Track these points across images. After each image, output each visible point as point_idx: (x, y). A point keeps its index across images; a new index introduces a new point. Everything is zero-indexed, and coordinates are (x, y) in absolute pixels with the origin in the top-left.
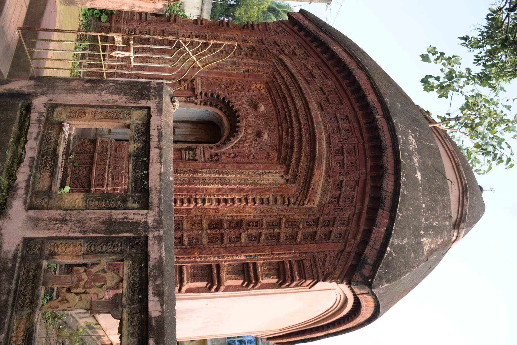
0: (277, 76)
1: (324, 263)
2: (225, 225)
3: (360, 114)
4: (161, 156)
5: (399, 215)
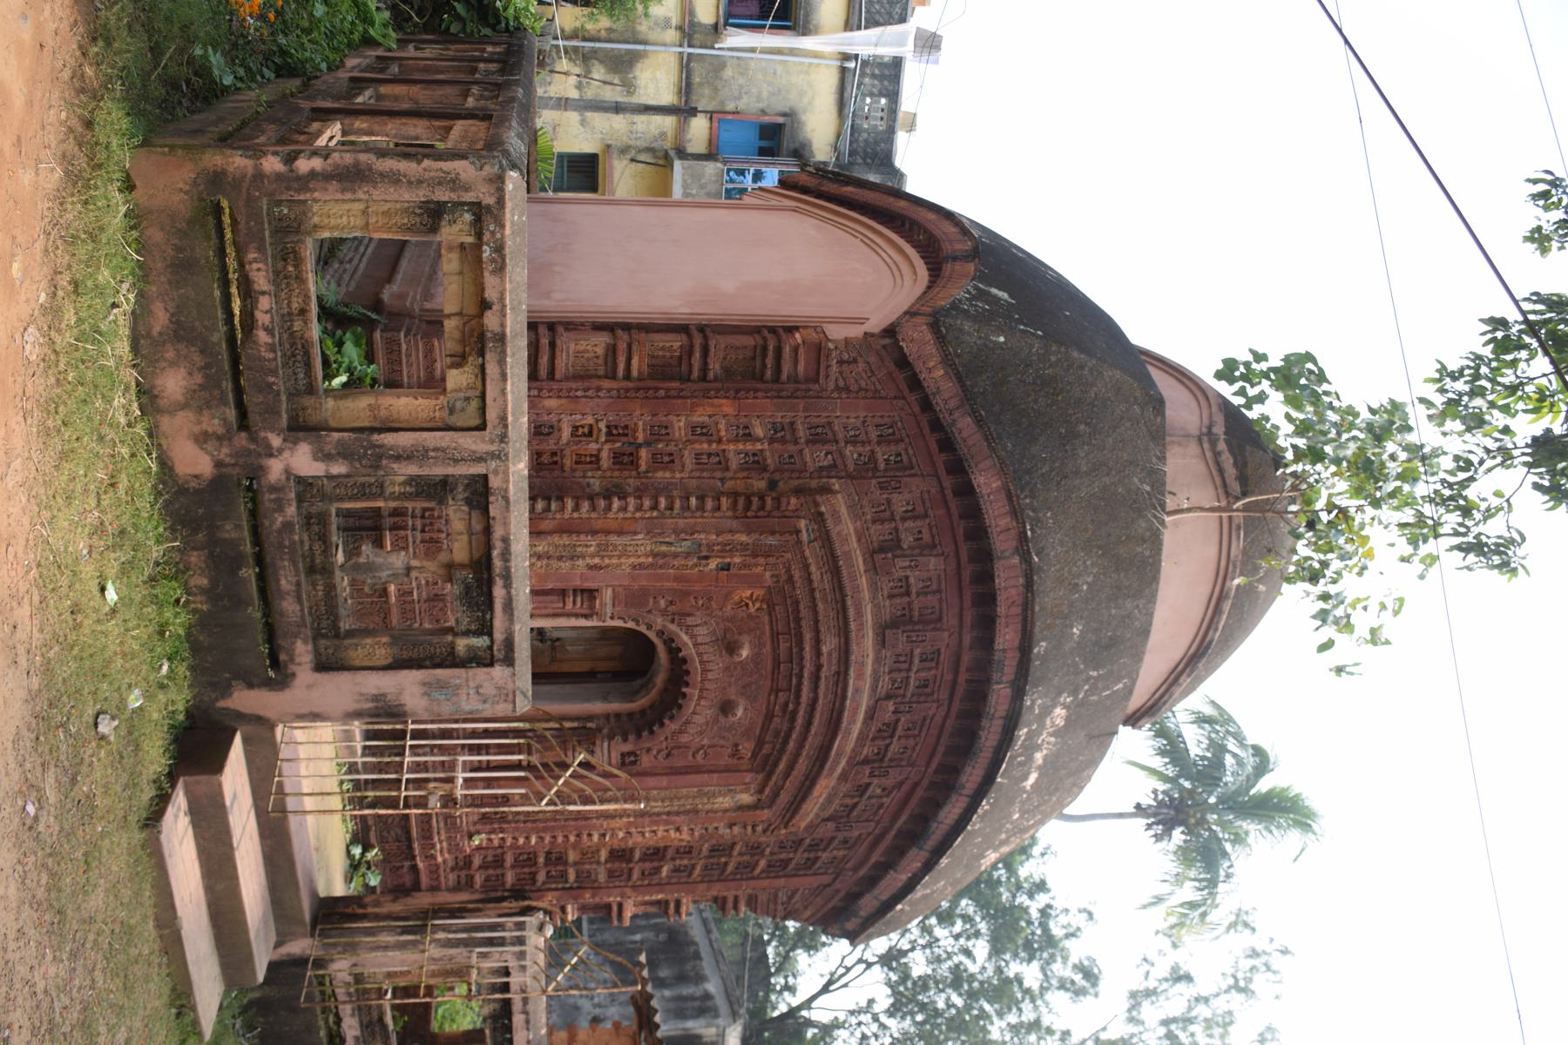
0: (797, 575)
1: (790, 898)
2: (637, 855)
3: (966, 659)
4: (527, 1022)
5: (944, 861)
